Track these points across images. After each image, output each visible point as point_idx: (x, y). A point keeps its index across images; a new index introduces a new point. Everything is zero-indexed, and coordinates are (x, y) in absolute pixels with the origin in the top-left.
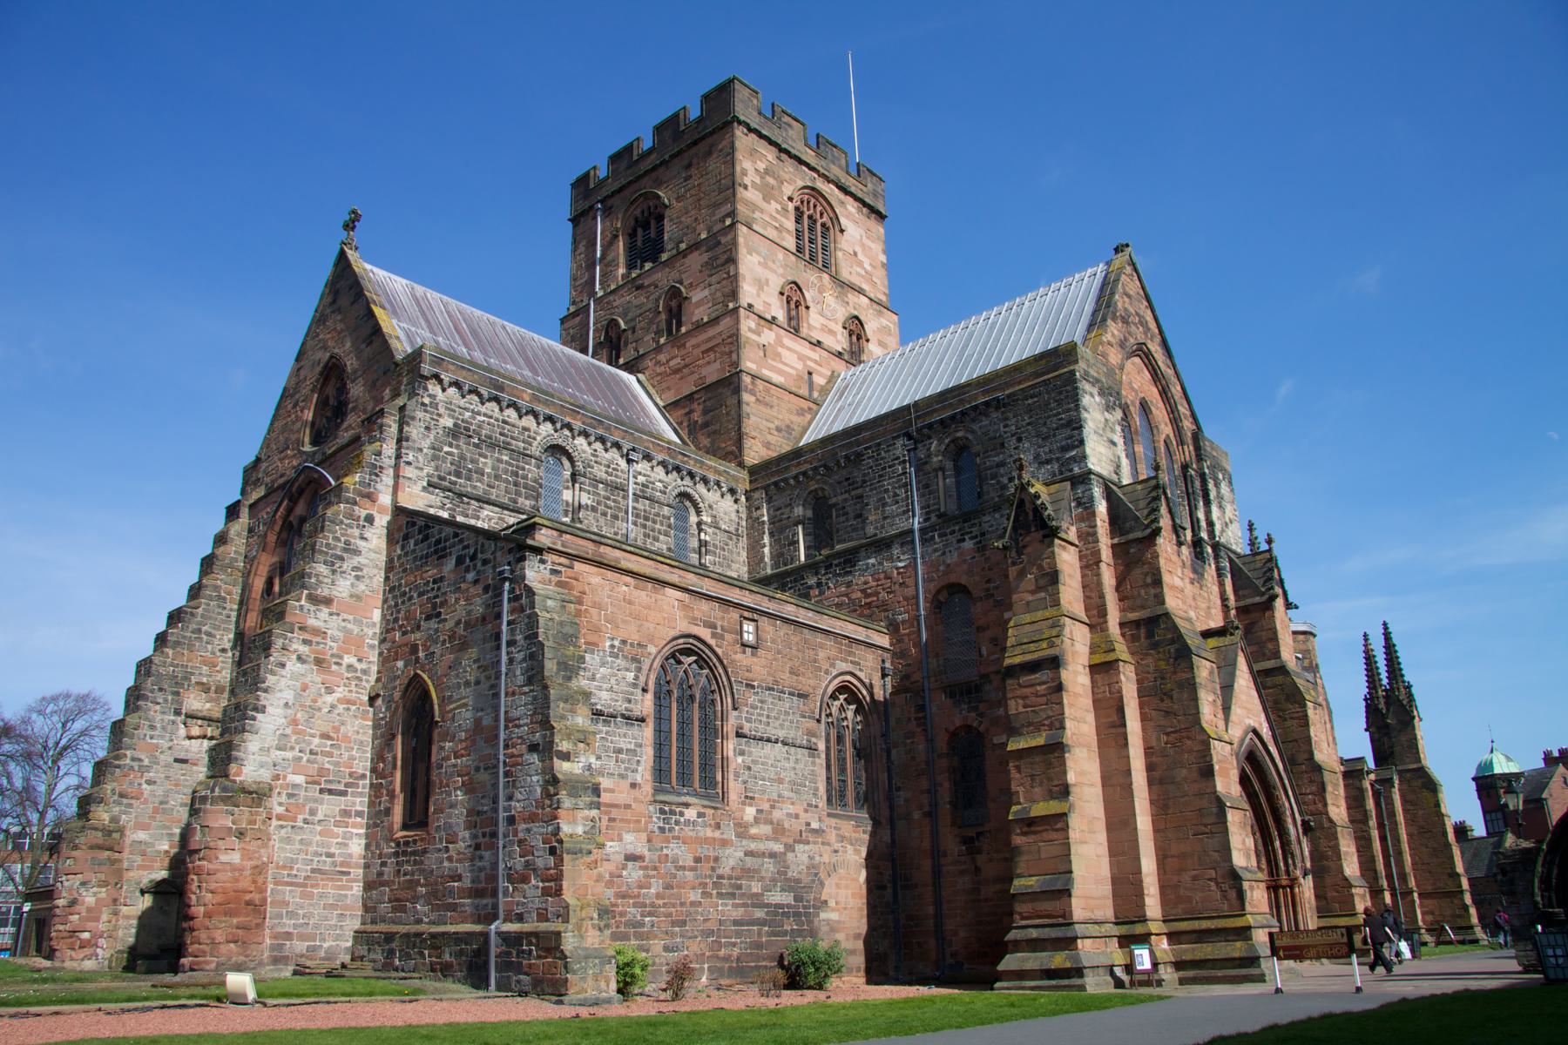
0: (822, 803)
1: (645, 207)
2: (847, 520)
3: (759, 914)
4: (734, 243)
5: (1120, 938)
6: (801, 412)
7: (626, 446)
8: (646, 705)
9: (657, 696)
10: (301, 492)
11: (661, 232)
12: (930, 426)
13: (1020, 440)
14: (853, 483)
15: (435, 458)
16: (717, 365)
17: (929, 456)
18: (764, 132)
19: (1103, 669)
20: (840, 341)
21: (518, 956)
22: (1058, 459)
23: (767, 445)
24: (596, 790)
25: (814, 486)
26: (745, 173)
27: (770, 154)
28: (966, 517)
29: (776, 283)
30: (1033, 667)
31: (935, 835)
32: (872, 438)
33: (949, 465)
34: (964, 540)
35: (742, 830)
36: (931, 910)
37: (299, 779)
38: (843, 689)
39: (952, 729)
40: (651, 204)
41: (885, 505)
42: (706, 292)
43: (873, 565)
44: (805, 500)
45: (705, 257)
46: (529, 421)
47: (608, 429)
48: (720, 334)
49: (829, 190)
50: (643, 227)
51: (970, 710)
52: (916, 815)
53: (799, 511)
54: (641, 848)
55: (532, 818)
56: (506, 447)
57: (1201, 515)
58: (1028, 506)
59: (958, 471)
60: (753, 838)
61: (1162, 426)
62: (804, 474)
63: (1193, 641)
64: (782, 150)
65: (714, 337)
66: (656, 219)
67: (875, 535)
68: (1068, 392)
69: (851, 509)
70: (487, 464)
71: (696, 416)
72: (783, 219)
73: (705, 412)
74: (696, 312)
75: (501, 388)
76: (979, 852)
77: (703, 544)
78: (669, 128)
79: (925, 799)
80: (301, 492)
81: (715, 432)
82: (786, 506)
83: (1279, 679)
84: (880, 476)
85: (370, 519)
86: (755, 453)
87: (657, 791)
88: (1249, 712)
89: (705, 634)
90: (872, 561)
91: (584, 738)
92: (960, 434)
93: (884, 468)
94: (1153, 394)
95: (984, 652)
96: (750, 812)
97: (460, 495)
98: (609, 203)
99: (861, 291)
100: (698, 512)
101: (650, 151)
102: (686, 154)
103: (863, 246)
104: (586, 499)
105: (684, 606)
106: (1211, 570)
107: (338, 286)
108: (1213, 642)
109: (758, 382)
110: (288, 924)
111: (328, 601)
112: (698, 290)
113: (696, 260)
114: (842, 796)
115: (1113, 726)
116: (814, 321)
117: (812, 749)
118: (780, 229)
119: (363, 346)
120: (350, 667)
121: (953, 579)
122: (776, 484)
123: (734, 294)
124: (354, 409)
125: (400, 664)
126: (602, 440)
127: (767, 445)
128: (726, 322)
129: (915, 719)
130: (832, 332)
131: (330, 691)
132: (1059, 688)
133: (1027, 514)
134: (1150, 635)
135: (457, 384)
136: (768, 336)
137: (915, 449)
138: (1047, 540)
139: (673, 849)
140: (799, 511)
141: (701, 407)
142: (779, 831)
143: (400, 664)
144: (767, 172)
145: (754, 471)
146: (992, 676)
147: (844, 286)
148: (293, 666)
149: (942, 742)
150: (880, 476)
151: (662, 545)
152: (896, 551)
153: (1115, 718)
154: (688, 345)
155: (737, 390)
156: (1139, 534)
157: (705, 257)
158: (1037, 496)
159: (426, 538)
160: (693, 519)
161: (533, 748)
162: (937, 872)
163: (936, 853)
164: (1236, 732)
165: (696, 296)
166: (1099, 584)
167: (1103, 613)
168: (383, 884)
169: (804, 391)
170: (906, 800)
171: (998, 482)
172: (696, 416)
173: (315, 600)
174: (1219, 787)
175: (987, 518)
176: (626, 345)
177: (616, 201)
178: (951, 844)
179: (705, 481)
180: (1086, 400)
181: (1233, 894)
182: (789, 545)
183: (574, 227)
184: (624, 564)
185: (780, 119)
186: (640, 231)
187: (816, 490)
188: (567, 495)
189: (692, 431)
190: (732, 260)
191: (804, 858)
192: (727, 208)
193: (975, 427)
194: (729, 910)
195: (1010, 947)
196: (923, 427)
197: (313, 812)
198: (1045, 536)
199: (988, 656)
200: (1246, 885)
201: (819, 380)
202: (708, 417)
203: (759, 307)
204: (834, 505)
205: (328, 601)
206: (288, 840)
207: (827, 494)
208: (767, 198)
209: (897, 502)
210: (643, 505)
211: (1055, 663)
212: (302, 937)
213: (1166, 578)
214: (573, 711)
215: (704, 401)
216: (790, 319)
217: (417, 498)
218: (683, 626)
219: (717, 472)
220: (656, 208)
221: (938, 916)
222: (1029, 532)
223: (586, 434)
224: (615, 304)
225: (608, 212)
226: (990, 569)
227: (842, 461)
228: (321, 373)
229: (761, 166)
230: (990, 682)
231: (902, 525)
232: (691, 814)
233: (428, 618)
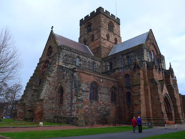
3: (102, 115)
4: (100, 29)
5: (147, 120)
6: (109, 51)
7: (87, 56)
8: (89, 90)
9: (90, 88)
11: (91, 28)
15: (63, 59)
16: (98, 45)
19: (145, 85)
20: (114, 41)
23: (104, 55)
24: (83, 100)
26: (102, 20)
29: (106, 34)
30: (136, 85)
32: (117, 55)
33: (127, 59)
35: (100, 105)
36: (124, 115)
37: (47, 98)
38: (113, 87)
45: (97, 31)
46: (75, 54)
47: (84, 54)
52: (122, 103)
53: (108, 64)
54: (88, 107)
55: (75, 104)
56: (72, 57)
57: (160, 65)
59: (128, 60)
60: (102, 106)
61: (155, 53)
62: (109, 59)
63: (158, 82)
64: (106, 16)
68: (142, 50)
69: (115, 64)
70: (69, 59)
71: (96, 52)
75: (70, 49)
77: (96, 68)
78: (93, 13)
80: (47, 62)
83: (170, 87)
85: (55, 66)
86: (103, 56)
87: (90, 100)
88: (165, 91)
89: (96, 81)
91: (81, 94)
94: (154, 49)
96: (101, 102)
97: (66, 63)
99: (117, 35)
100: (96, 64)
104: (82, 63)
105: (93, 78)
106: (161, 73)
108: (161, 82)
110: (46, 116)
111: (50, 77)
113: (95, 31)
114: (113, 100)
115: (147, 93)
116: (111, 39)
117: (109, 95)
120: (53, 84)
123: (100, 36)
125: (59, 84)
126: (84, 56)
127: (104, 55)
128: (99, 39)
131: (51, 87)
132: (140, 88)
135: (66, 49)
136: (105, 41)
139: (92, 107)
142: (105, 105)
143: (59, 84)
144: (105, 19)
145: (103, 59)
147: (115, 34)
148: (46, 85)
149: (125, 94)
151: (91, 69)
158: (137, 64)
159: (62, 69)
160: (95, 65)
161: (75, 95)
164: (163, 93)
166: (145, 75)
167: (146, 78)
168: (57, 111)
169: (109, 48)
172: (96, 52)
173: (49, 77)
174: (160, 101)
177: (85, 23)
179: (96, 60)
180: (144, 51)
184: (86, 73)
188: (79, 63)
189: (94, 53)
190: (100, 31)
191: (108, 108)
192: (99, 25)
194: (98, 114)
197: (49, 102)
200: (164, 114)
201: (111, 47)
203: (103, 37)
205: (50, 77)
206: (46, 106)
210: (89, 64)
211: (139, 85)
212: (48, 117)
213: (154, 74)
214: (80, 91)
216: (107, 39)
217: (61, 64)
218: (93, 80)
223: (82, 55)
225: (84, 24)
229: (104, 19)
232: (94, 103)
233: (63, 79)
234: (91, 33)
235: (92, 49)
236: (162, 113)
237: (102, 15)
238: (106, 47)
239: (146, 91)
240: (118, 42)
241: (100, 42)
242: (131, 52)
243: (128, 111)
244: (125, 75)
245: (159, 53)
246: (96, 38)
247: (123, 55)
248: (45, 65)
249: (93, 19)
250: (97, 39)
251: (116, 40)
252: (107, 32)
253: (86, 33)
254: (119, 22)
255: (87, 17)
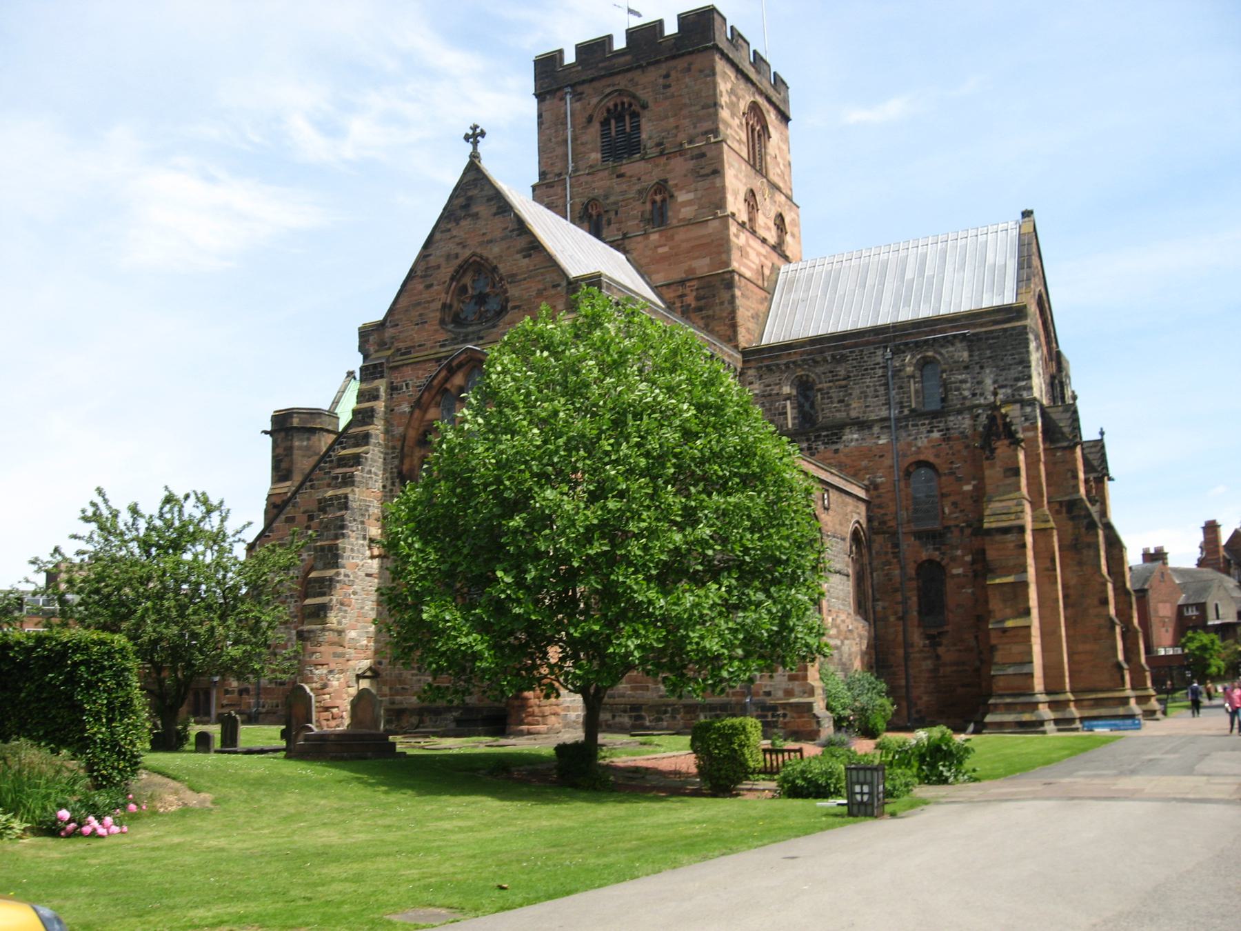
0: (852, 611)
1: (619, 101)
2: (832, 402)
10: (460, 366)
11: (637, 128)
12: (906, 344)
13: (982, 368)
14: (836, 375)
16: (707, 260)
17: (903, 365)
18: (731, 56)
20: (772, 238)
21: (773, 716)
22: (1012, 386)
23: (748, 330)
25: (800, 372)
27: (731, 73)
28: (935, 415)
31: (905, 632)
32: (856, 345)
33: (918, 374)
34: (932, 432)
36: (903, 682)
39: (920, 561)
40: (625, 100)
41: (866, 397)
42: (691, 196)
43: (857, 440)
44: (792, 383)
48: (710, 235)
49: (761, 101)
50: (615, 119)
51: (936, 549)
52: (892, 619)
53: (787, 390)
58: (999, 421)
62: (794, 363)
65: (703, 236)
66: (630, 115)
67: (858, 418)
69: (834, 394)
72: (740, 132)
73: (698, 299)
74: (683, 210)
76: (940, 644)
79: (900, 608)
80: (460, 366)
81: (708, 317)
82: (776, 384)
84: (863, 375)
90: (855, 436)
92: (930, 354)
93: (866, 370)
95: (947, 511)
98: (579, 89)
101: (621, 53)
102: (664, 65)
103: (779, 148)
107: (470, 193)
109: (742, 279)
112: (684, 191)
113: (679, 167)
115: (1047, 570)
117: (848, 576)
118: (740, 141)
119: (519, 256)
121: (922, 457)
122: (767, 366)
124: (514, 308)
129: (893, 553)
130: (769, 229)
133: (998, 427)
134: (1069, 511)
137: (891, 359)
138: (1012, 447)
140: (787, 390)
141: (694, 293)
146: (953, 529)
149: (911, 571)
150: (863, 375)
152: (876, 429)
153: (1049, 565)
154: (677, 238)
155: (730, 285)
156: (1065, 444)
157: (691, 164)
162: (907, 657)
163: (907, 645)
165: (682, 197)
169: (760, 283)
170: (884, 608)
171: (961, 394)
172: (690, 299)
175: (951, 418)
176: (609, 223)
177: (586, 89)
178: (917, 638)
181: (1118, 676)
182: (780, 414)
183: (539, 103)
185: (737, 41)
186: (613, 122)
187: (801, 376)
192: (707, 125)
193: (943, 351)
195: (991, 708)
196: (900, 344)
198: (1011, 444)
199: (951, 513)
201: (767, 272)
202: (702, 302)
204: (819, 390)
207: (811, 379)
208: (733, 115)
209: (877, 396)
215: (697, 289)
216: (750, 220)
219: (730, 356)
220: (630, 105)
221: (907, 687)
222: (999, 439)
224: (594, 185)
225: (578, 96)
226: (953, 454)
227: (829, 358)
228: (461, 267)
229: (729, 86)
230: (952, 532)
231: (884, 413)
234: (634, 167)
235: (660, 279)
236: (1119, 667)
237: (721, 65)
238: (748, 274)
239: (1045, 556)
240: (788, 238)
241: (722, 246)
242: (948, 341)
243: (928, 664)
244: (911, 465)
245: (1054, 345)
246: (687, 212)
247: (897, 352)
248: (446, 379)
249: (653, 75)
250: (690, 223)
251: (780, 221)
252: (747, 176)
253: (596, 156)
254: (786, 101)
255: (594, 50)
